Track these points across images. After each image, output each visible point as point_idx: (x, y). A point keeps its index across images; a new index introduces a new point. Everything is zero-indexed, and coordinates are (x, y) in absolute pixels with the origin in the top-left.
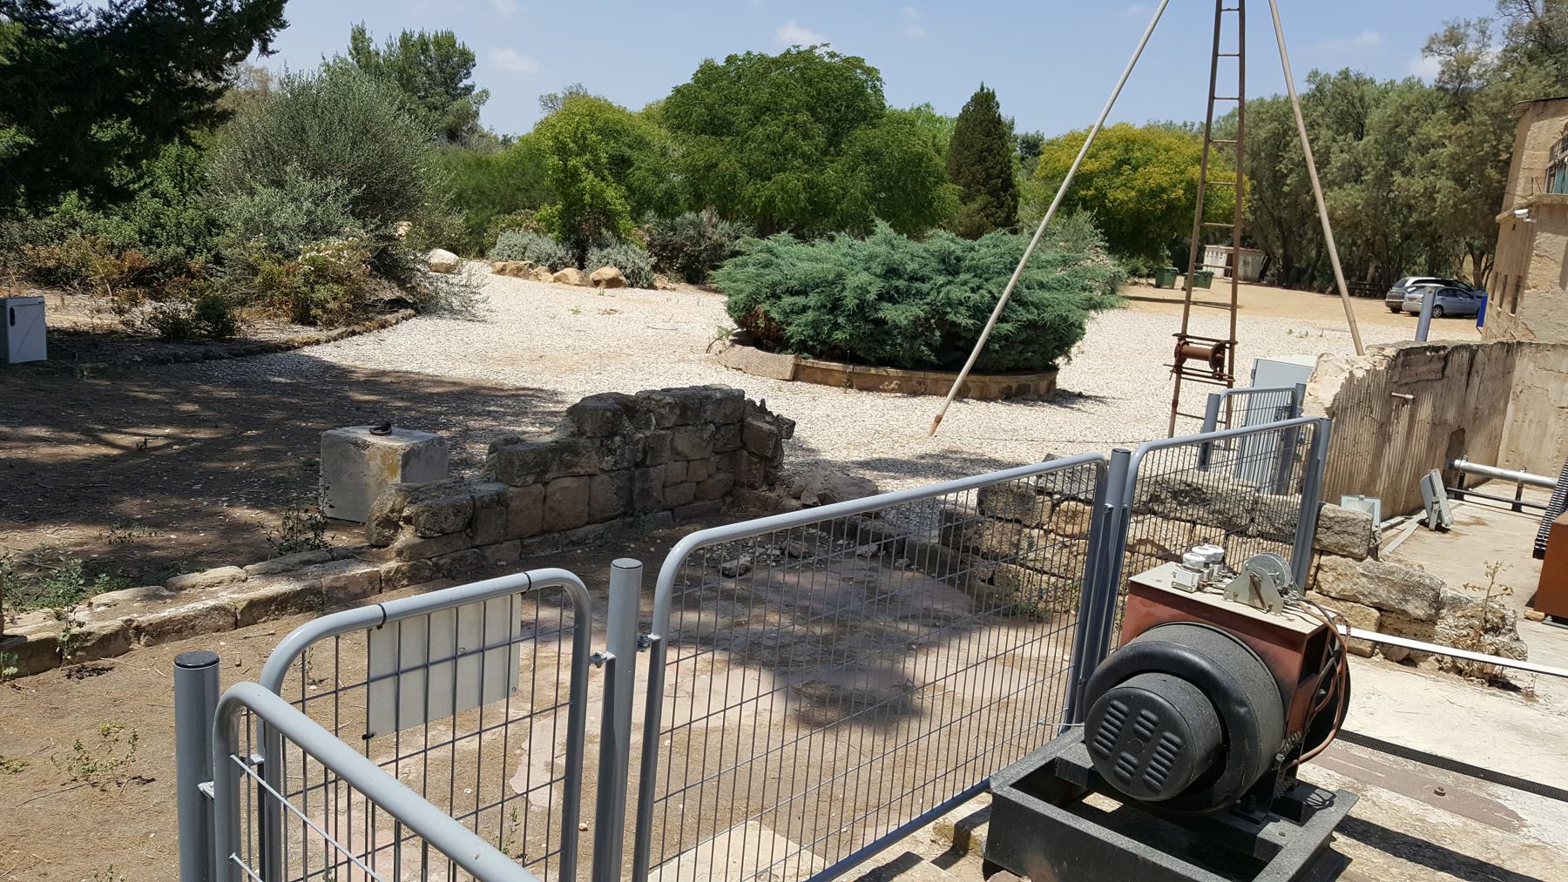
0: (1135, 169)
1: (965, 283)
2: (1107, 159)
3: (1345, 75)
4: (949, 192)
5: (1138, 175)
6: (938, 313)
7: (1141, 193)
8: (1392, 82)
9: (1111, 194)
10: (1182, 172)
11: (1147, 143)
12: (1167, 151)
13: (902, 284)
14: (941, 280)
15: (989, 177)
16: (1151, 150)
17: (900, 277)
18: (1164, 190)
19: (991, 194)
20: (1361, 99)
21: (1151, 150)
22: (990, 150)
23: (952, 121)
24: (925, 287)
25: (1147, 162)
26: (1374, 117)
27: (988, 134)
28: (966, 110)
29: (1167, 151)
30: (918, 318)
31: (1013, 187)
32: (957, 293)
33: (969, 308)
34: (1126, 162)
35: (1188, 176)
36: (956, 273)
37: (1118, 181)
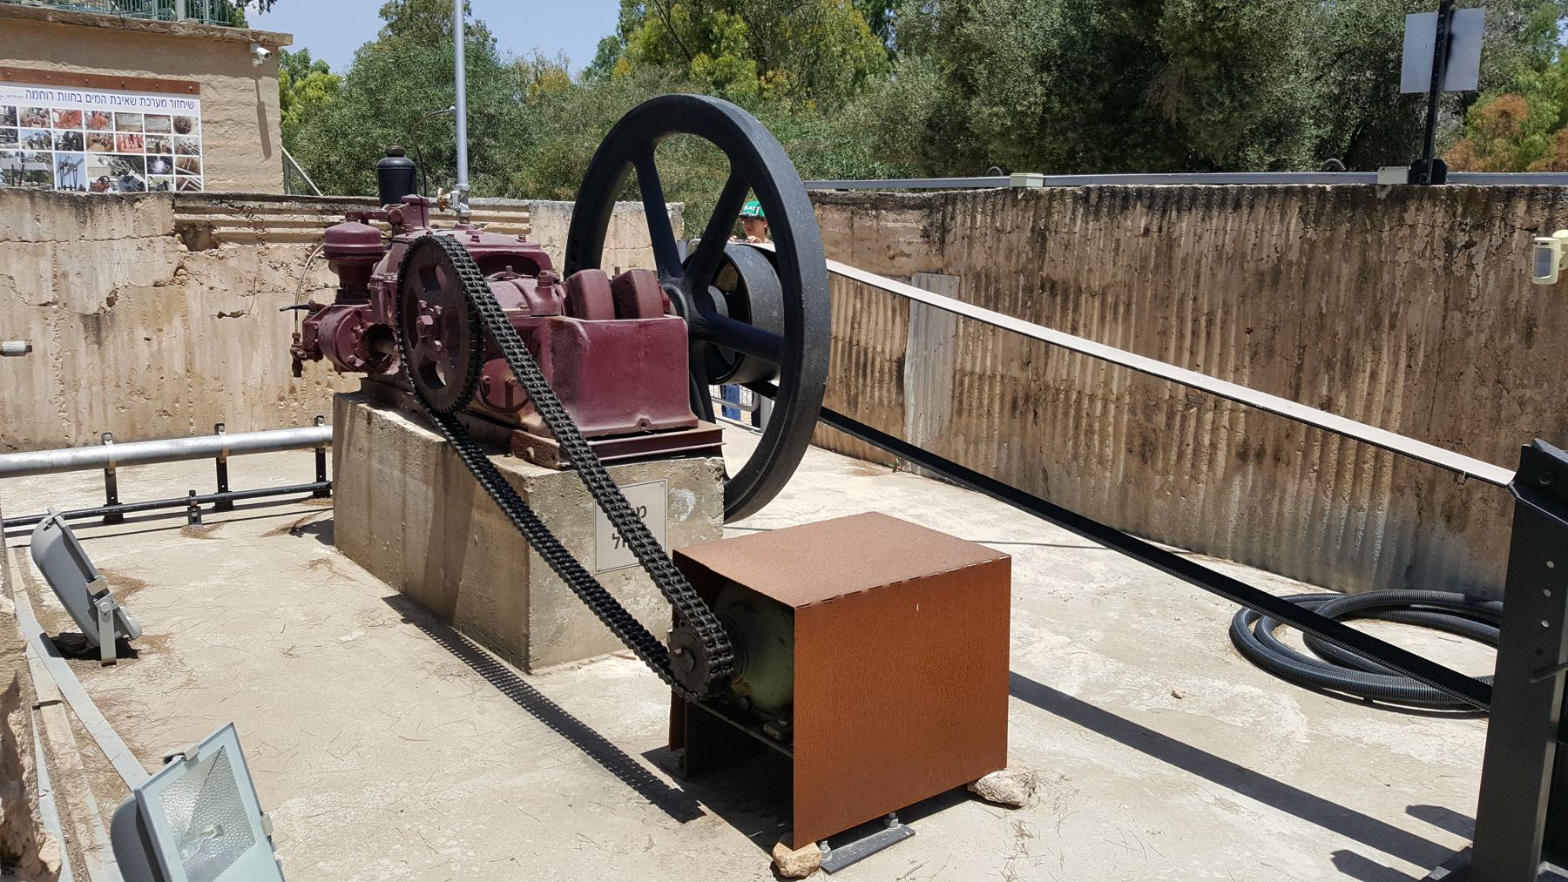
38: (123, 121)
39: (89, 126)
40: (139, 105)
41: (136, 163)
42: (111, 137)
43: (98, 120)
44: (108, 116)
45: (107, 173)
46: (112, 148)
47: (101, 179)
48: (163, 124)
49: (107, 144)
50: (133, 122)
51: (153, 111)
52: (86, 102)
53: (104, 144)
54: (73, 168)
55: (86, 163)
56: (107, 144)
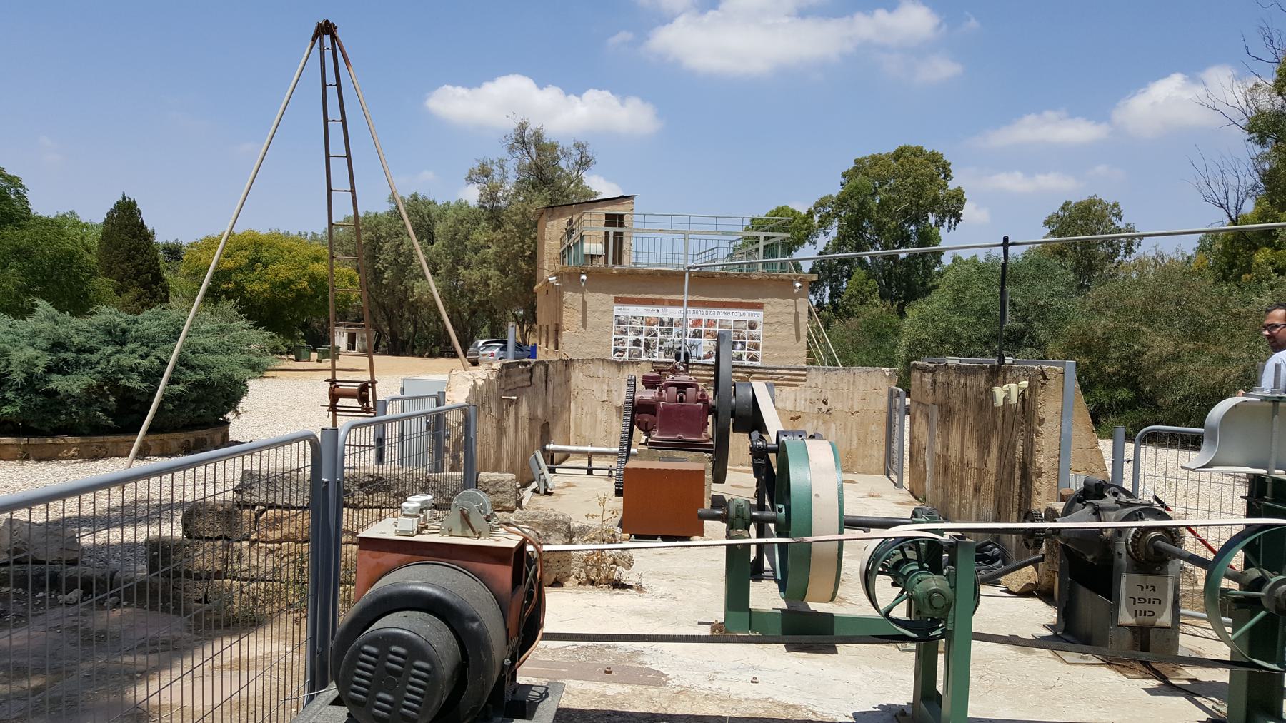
0: (266, 266)
1: (133, 351)
2: (241, 258)
3: (415, 197)
4: (104, 284)
5: (269, 271)
6: (111, 381)
7: (273, 284)
8: (448, 203)
9: (248, 287)
10: (304, 268)
11: (272, 246)
12: (290, 252)
13: (70, 356)
14: (109, 349)
15: (139, 272)
16: (276, 251)
17: (67, 350)
18: (291, 282)
19: (144, 285)
20: (429, 216)
21: (276, 251)
22: (137, 249)
23: (98, 226)
24: (95, 357)
25: (275, 260)
26: (439, 228)
27: (134, 236)
28: (110, 215)
29: (290, 252)
30: (90, 386)
31: (163, 280)
32: (126, 360)
33: (140, 374)
34: (258, 260)
35: (309, 271)
36: (124, 343)
37: (253, 276)
40: (731, 315)
43: (710, 323)
48: (743, 325)
52: (705, 314)
54: (696, 347)
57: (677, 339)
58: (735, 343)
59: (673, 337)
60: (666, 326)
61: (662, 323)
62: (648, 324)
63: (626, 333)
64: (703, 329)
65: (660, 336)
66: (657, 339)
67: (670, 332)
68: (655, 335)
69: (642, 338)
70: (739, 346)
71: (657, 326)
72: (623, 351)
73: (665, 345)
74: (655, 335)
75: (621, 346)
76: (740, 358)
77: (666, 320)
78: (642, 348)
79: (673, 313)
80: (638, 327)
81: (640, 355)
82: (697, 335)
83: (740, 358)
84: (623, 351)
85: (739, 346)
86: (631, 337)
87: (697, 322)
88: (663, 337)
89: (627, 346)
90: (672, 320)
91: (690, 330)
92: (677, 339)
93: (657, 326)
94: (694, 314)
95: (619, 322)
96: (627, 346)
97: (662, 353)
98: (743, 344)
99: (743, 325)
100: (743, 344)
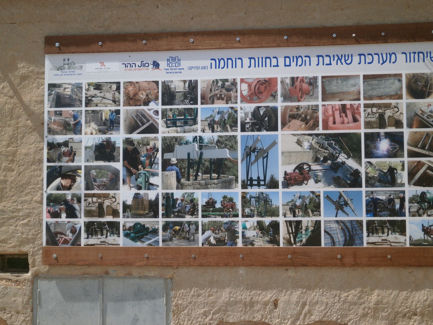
38: (334, 87)
39: (286, 97)
40: (357, 64)
41: (349, 143)
42: (315, 109)
43: (298, 88)
44: (312, 82)
45: (308, 158)
46: (315, 125)
47: (300, 168)
49: (309, 119)
50: (347, 87)
51: (376, 69)
53: (305, 120)
55: (280, 147)
56: (309, 119)
57: (208, 136)
58: (372, 138)
59: (200, 130)
60: (182, 102)
61: (169, 96)
62: (131, 100)
63: (76, 128)
64: (280, 104)
65: (164, 132)
66: (157, 140)
67: (189, 118)
68: (153, 129)
69: (118, 138)
70: (384, 145)
71: (157, 106)
72: (71, 175)
73: (179, 153)
74: (153, 129)
75: (65, 163)
76: (389, 178)
77: (178, 86)
78: (119, 165)
79: (197, 68)
80: (106, 110)
81: (113, 183)
82: (265, 121)
83: (389, 178)
84: (71, 175)
85: (384, 145)
86: (89, 137)
87: (263, 88)
88: (172, 133)
89: (81, 161)
90: (193, 86)
91: (245, 110)
92: (208, 136)
93: (157, 106)
94: (245, 68)
95: (60, 101)
96: (81, 161)
97: (172, 175)
98: (396, 139)
99: (391, 87)
100: (396, 139)
